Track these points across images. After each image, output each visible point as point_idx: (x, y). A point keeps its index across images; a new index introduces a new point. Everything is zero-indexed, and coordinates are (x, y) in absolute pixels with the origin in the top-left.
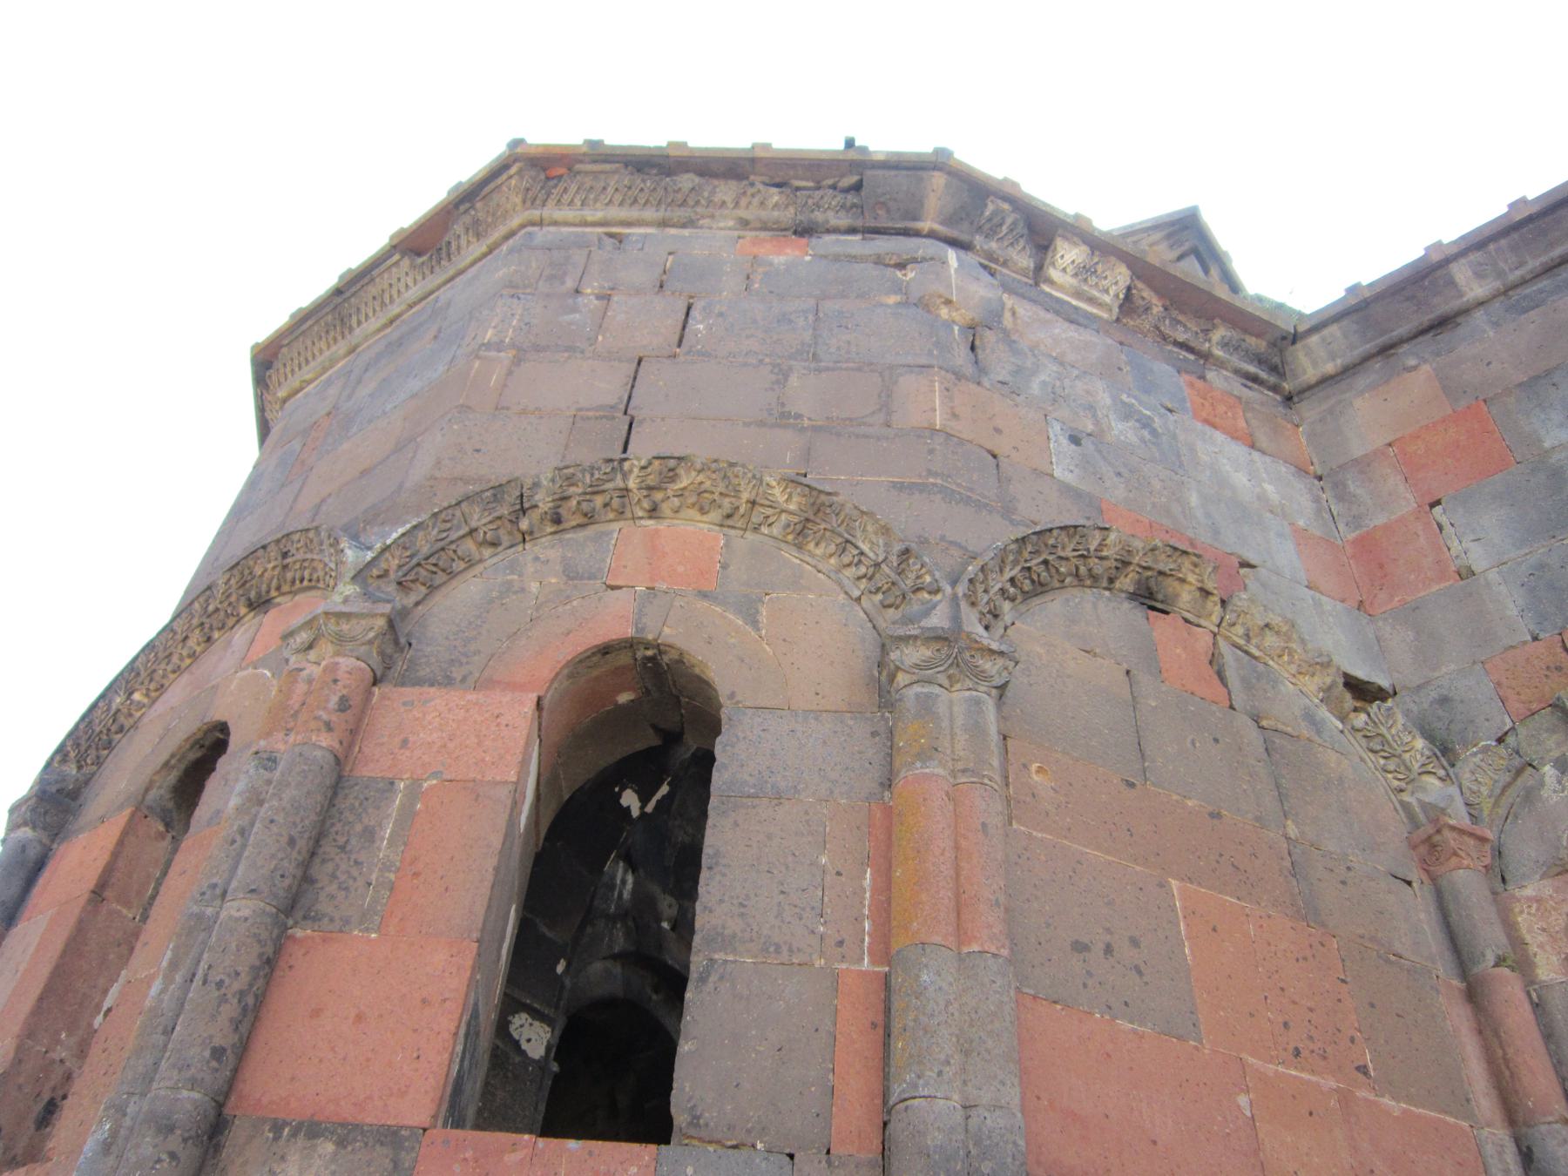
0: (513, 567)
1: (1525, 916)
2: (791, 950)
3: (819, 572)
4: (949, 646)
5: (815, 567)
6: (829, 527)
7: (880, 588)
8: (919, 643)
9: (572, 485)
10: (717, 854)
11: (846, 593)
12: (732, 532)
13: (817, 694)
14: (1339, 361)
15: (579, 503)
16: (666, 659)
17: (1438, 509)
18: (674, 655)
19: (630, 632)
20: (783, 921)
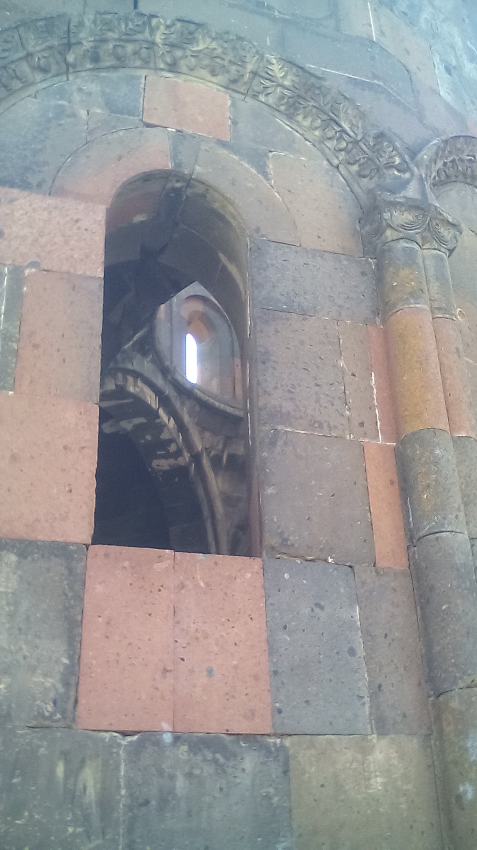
0: (62, 93)
2: (329, 426)
3: (306, 139)
4: (424, 215)
5: (302, 135)
9: (110, 30)
10: (267, 352)
11: (328, 160)
12: (236, 95)
13: (319, 237)
15: (114, 47)
16: (189, 192)
18: (200, 189)
19: (170, 166)
20: (321, 406)
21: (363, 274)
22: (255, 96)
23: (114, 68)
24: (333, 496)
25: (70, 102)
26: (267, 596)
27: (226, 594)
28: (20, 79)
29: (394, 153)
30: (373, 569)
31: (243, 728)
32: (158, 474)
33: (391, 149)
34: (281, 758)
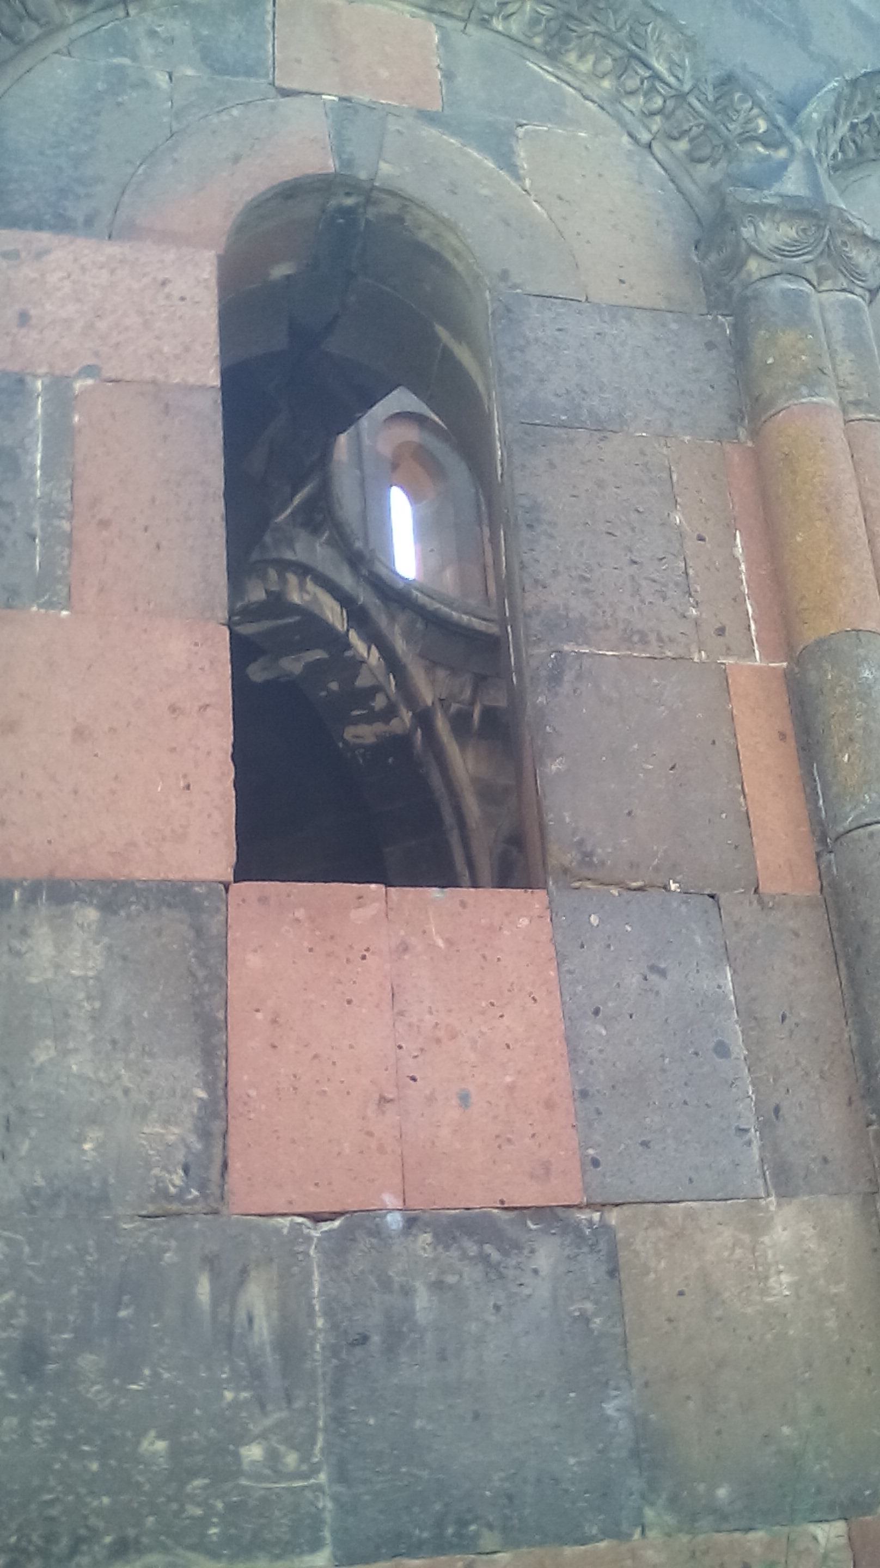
0: (118, 43)
2: (660, 639)
4: (819, 227)
7: (686, 132)
8: (778, 217)
11: (631, 135)
12: (448, 23)
13: (622, 282)
16: (371, 212)
18: (391, 207)
19: (331, 165)
20: (643, 601)
21: (710, 346)
22: (484, 23)
24: (672, 768)
25: (135, 58)
26: (560, 958)
27: (484, 957)
29: (756, 111)
30: (754, 898)
31: (530, 1195)
32: (356, 752)
33: (749, 104)
34: (602, 1245)
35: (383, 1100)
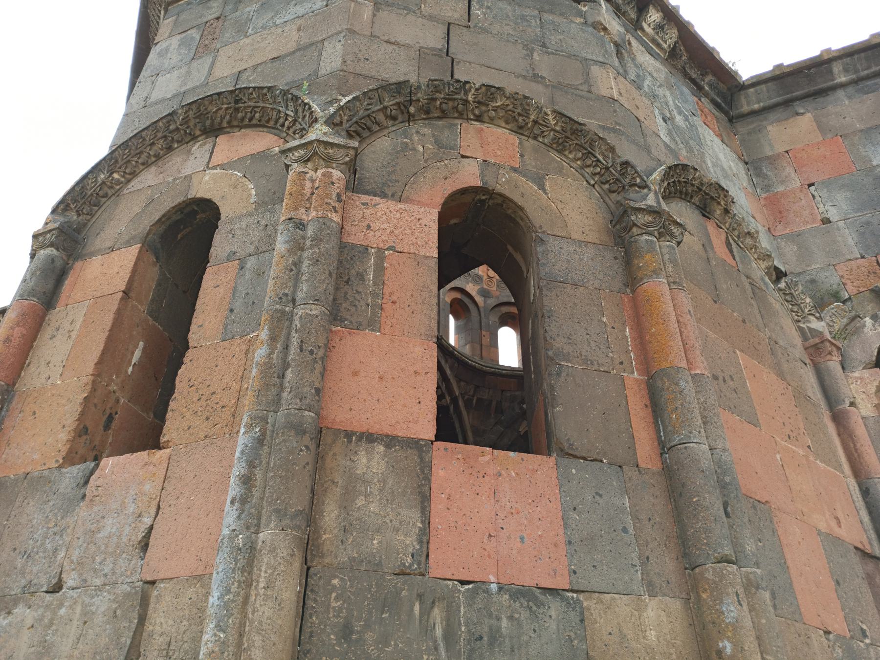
0: (405, 135)
1: (854, 385)
2: (598, 364)
3: (571, 167)
4: (660, 217)
5: (568, 164)
6: (579, 143)
7: (609, 181)
8: (645, 213)
9: (437, 92)
11: (587, 181)
14: (762, 104)
15: (441, 103)
17: (812, 188)
18: (499, 200)
20: (591, 349)
21: (616, 258)
22: (535, 138)
23: (440, 118)
25: (411, 140)
26: (561, 486)
28: (378, 125)
29: (636, 175)
30: (637, 469)
33: (633, 172)
35: (490, 536)
